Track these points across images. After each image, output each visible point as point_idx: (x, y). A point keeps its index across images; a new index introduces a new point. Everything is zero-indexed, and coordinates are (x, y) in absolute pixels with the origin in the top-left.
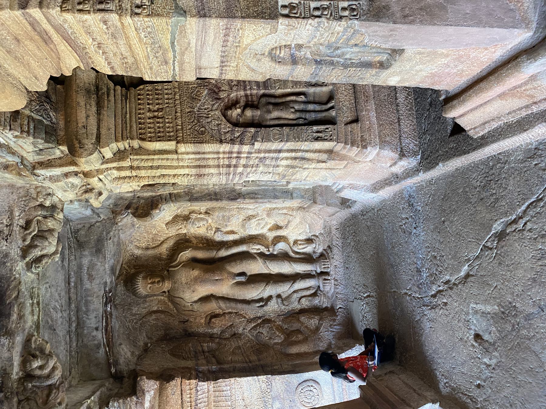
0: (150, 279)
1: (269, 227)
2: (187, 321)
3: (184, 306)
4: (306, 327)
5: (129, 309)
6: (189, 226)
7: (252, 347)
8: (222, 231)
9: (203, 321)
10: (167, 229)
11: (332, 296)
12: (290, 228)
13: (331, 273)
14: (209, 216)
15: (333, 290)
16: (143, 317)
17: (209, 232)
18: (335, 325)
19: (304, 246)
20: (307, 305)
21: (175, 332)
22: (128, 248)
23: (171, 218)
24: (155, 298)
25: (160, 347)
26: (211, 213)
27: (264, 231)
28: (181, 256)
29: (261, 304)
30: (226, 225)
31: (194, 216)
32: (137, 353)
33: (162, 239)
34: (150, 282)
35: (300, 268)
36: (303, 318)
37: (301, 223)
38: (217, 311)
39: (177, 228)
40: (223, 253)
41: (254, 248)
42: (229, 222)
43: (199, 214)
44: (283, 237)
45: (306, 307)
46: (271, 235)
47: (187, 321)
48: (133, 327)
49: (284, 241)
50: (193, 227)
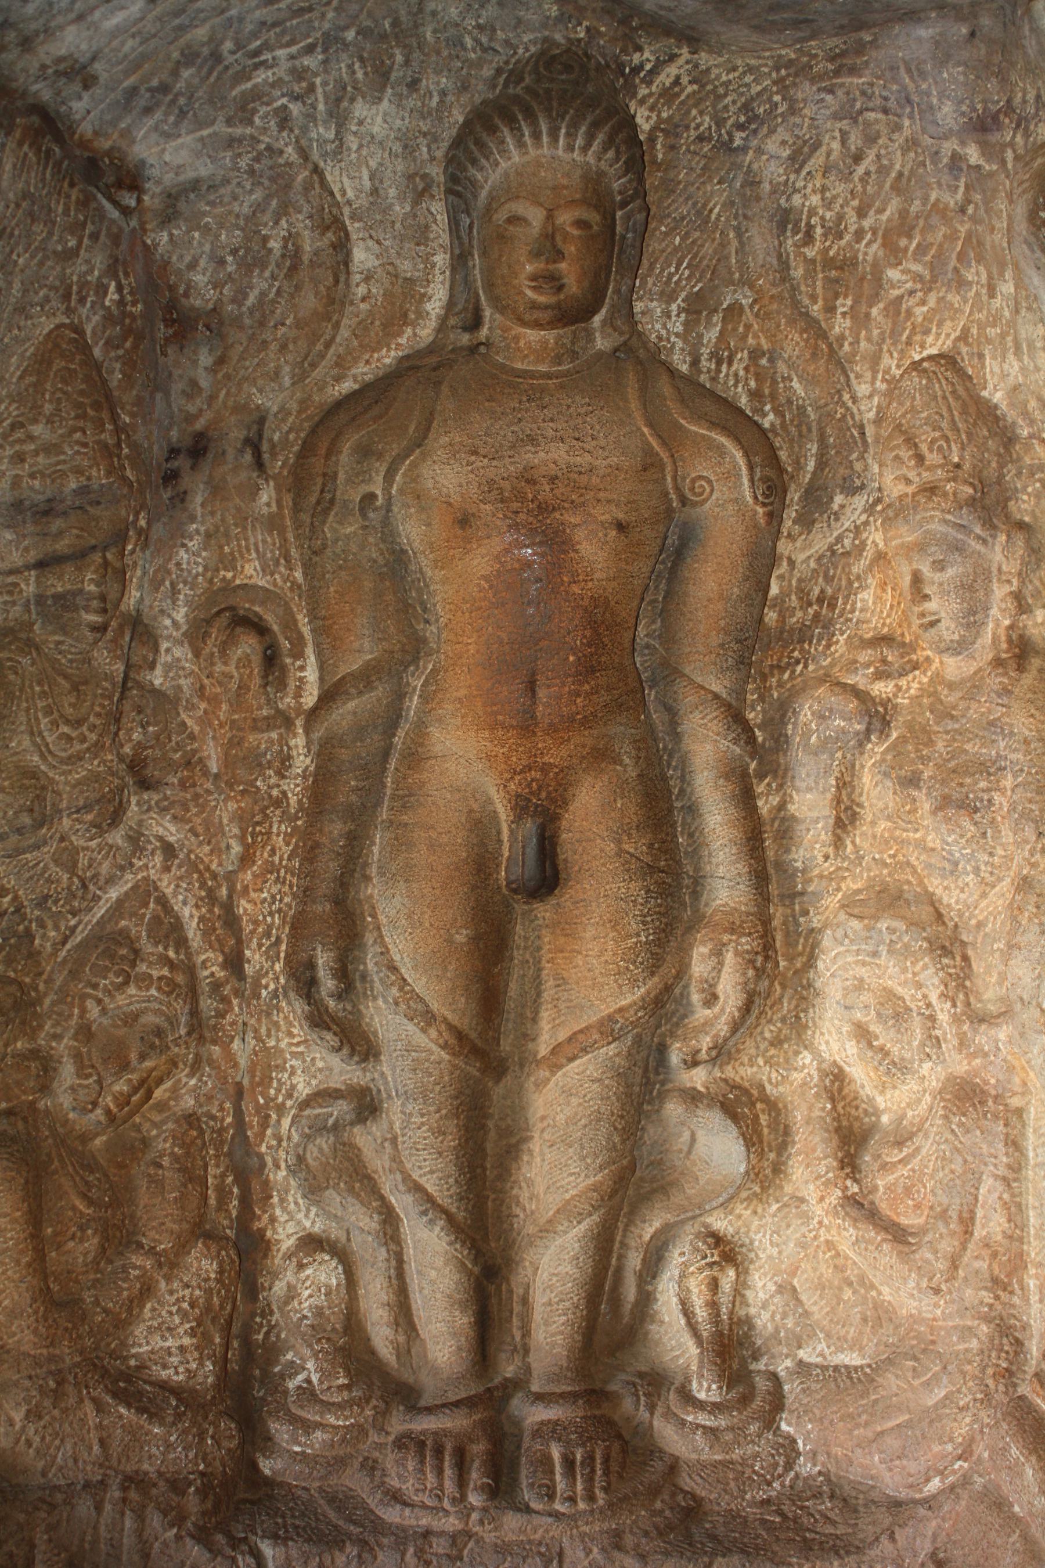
0: (580, 224)
1: (861, 1075)
2: (259, 465)
3: (365, 452)
4: (147, 1291)
5: (382, 76)
6: (936, 520)
7: (42, 902)
8: (861, 744)
9: (251, 572)
10: (916, 365)
11: (341, 1501)
12: (847, 1235)
13: (512, 1522)
14: (998, 662)
15: (392, 1515)
16: (316, 170)
17: (865, 656)
18: (140, 1517)
19: (701, 1313)
20: (292, 1293)
21: (194, 383)
22: (805, 90)
23: (998, 397)
24: (441, 259)
25: (111, 271)
26: (1028, 679)
27: (832, 1040)
28: (720, 450)
29: (328, 983)
30: (913, 781)
31: (1002, 555)
32: (78, 107)
33: (840, 325)
34: (565, 218)
35: (551, 1273)
36: (209, 1267)
37: (880, 1315)
38: (311, 674)
39: (925, 437)
40: (706, 747)
41: (717, 974)
42: (944, 803)
43: (1018, 597)
44: (778, 1169)
45: (279, 1288)
46: (794, 1080)
47: (259, 465)
48: (257, 95)
49: (753, 1174)
50: (921, 547)
